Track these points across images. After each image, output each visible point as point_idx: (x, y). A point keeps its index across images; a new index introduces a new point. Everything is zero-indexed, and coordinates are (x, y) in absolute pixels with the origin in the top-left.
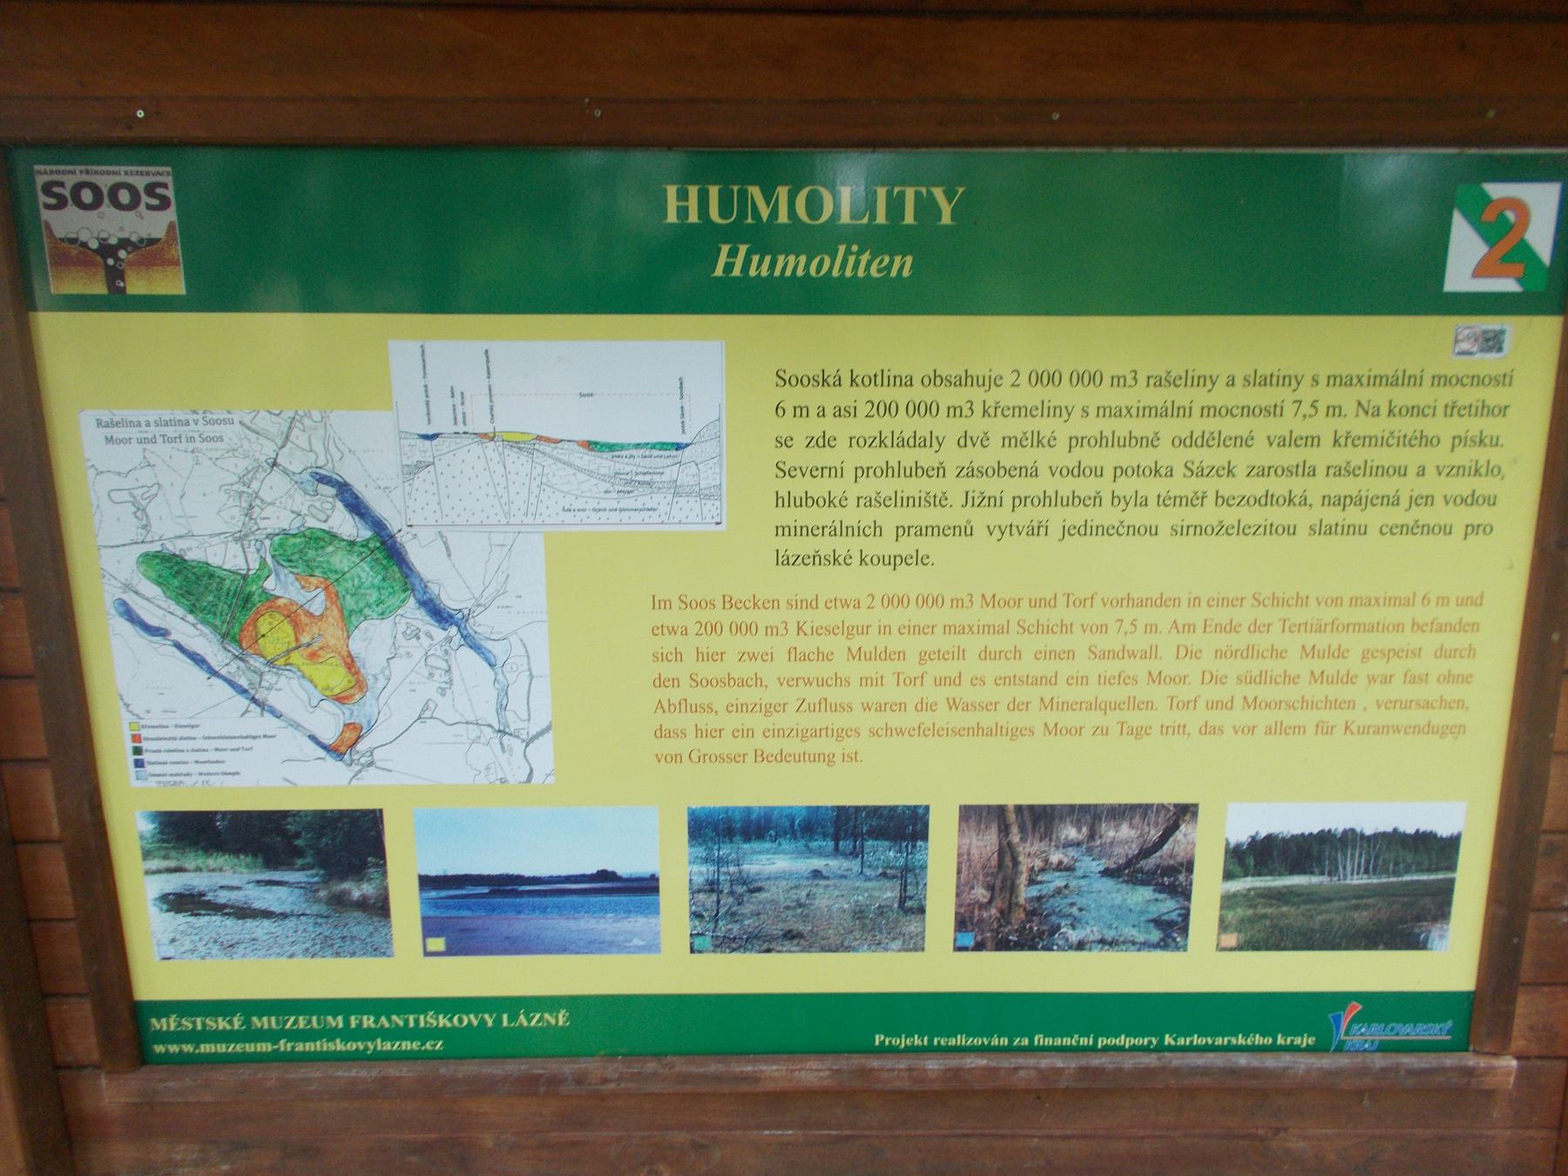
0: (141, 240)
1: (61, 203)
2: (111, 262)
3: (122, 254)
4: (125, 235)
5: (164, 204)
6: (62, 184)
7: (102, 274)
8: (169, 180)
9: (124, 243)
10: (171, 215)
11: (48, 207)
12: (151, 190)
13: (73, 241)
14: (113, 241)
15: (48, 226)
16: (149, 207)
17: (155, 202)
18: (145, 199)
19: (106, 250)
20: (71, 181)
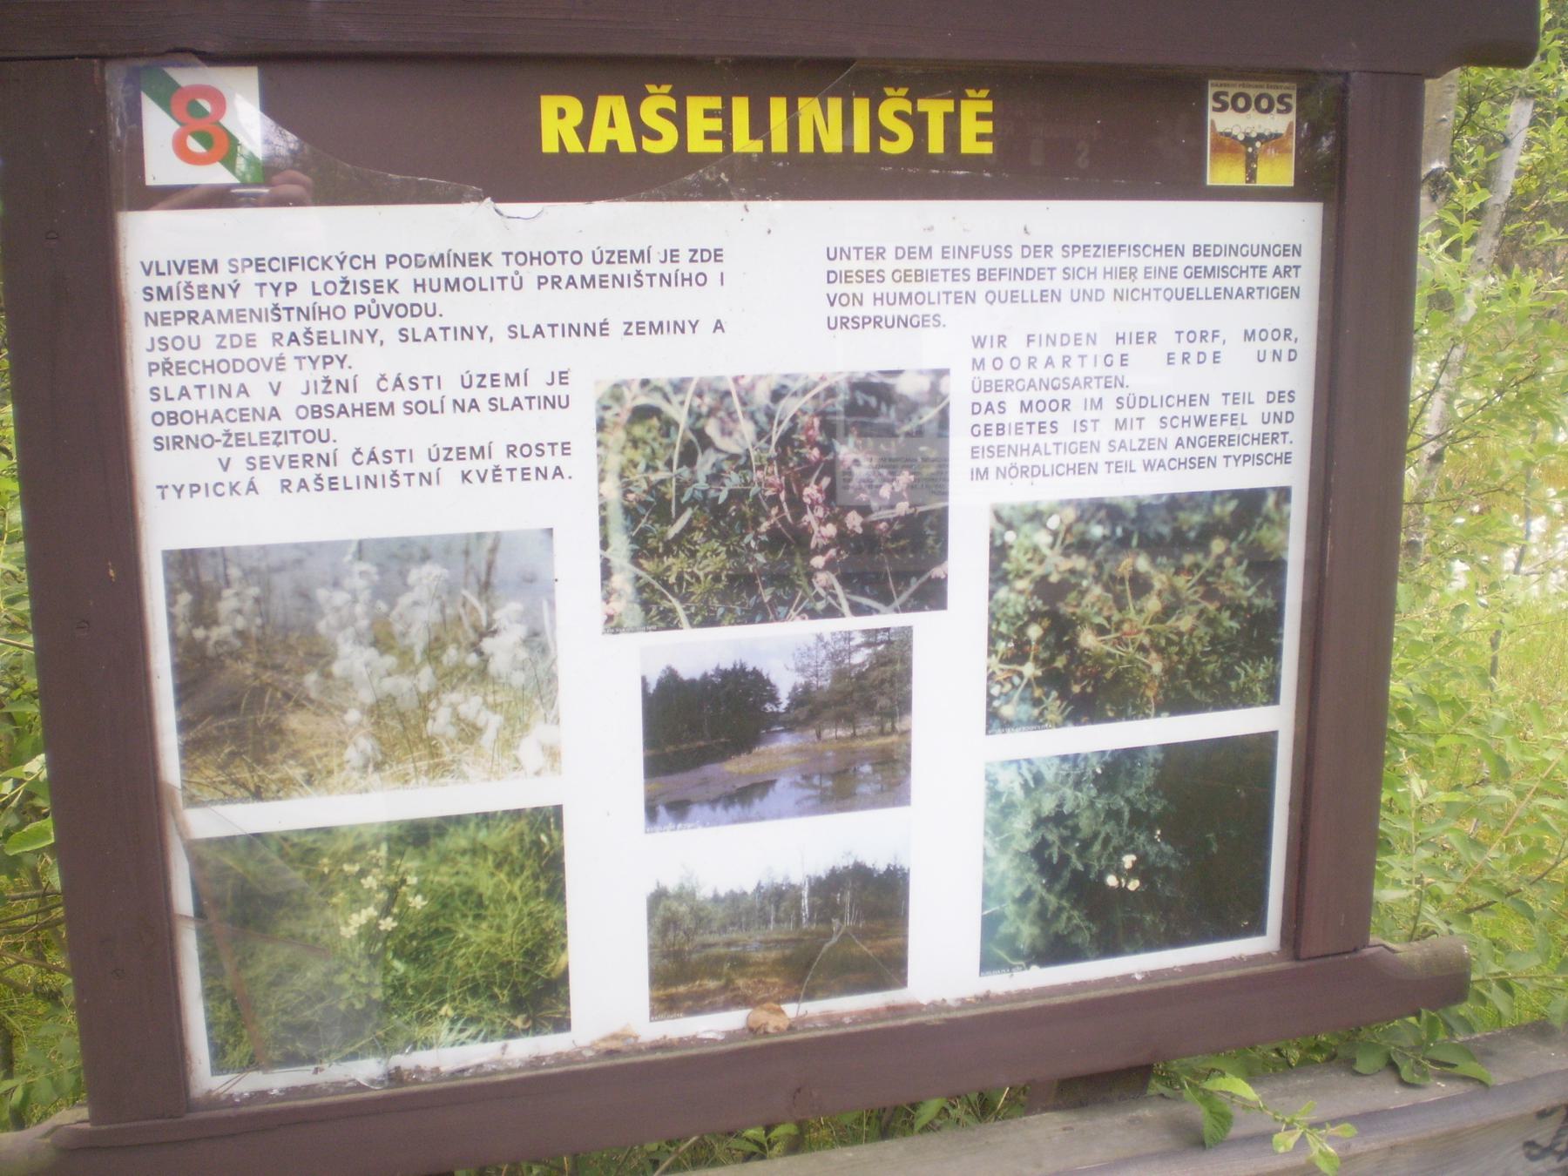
0: (1271, 135)
1: (1224, 108)
2: (1250, 150)
3: (1258, 144)
4: (1261, 131)
5: (1288, 110)
6: (1226, 94)
7: (1243, 159)
8: (1294, 93)
9: (1260, 137)
10: (1291, 117)
11: (1215, 109)
12: (1281, 99)
13: (1228, 135)
14: (1254, 135)
15: (1213, 123)
16: (1280, 112)
17: (1283, 108)
18: (1277, 106)
19: (1248, 141)
20: (1232, 92)
